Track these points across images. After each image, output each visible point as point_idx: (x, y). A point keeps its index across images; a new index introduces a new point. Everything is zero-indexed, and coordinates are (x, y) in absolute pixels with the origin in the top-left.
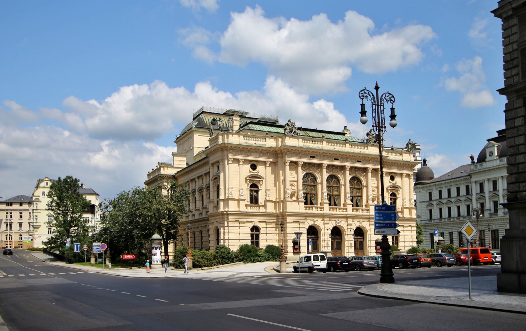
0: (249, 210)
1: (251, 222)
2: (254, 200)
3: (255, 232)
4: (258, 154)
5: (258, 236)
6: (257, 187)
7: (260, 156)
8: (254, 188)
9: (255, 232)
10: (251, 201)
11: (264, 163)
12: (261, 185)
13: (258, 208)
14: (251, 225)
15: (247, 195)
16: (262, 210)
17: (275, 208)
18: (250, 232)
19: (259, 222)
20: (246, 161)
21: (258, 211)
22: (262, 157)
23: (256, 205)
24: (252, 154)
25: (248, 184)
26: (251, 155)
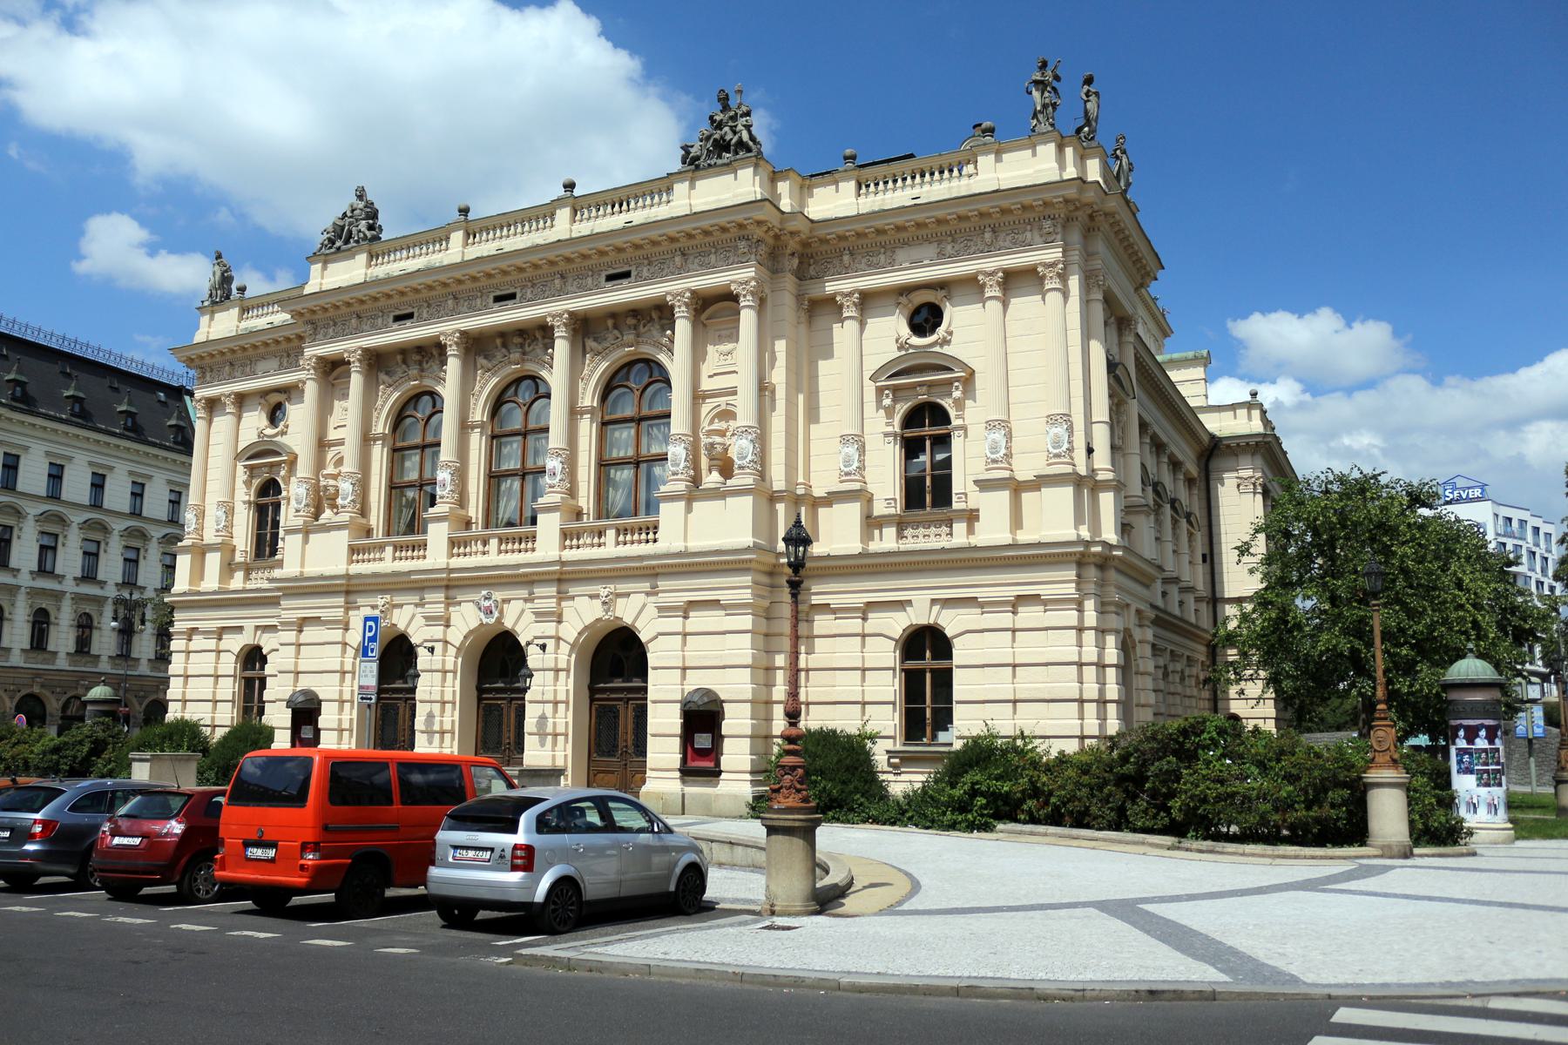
0: (887, 540)
1: (902, 605)
2: (928, 492)
3: (928, 662)
4: (932, 250)
5: (944, 681)
6: (941, 416)
7: (942, 257)
8: (925, 429)
9: (928, 662)
10: (914, 493)
11: (971, 287)
12: (959, 405)
13: (945, 529)
14: (898, 624)
15: (885, 476)
16: (959, 536)
17: (1078, 521)
18: (887, 654)
19: (947, 603)
20: (868, 301)
21: (945, 543)
22: (955, 256)
23: (941, 512)
24: (901, 254)
25: (890, 412)
26: (891, 265)
